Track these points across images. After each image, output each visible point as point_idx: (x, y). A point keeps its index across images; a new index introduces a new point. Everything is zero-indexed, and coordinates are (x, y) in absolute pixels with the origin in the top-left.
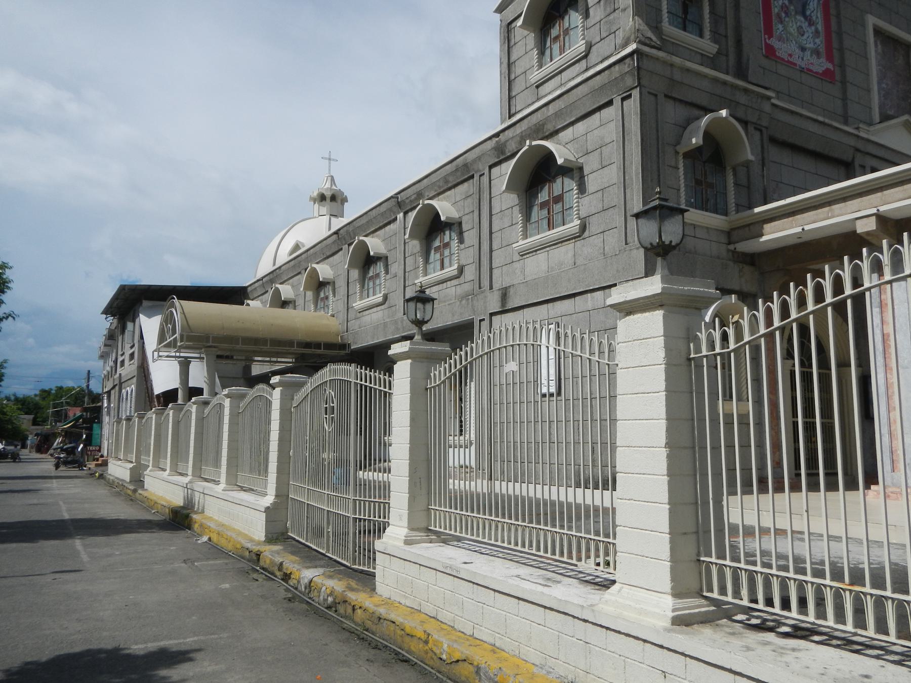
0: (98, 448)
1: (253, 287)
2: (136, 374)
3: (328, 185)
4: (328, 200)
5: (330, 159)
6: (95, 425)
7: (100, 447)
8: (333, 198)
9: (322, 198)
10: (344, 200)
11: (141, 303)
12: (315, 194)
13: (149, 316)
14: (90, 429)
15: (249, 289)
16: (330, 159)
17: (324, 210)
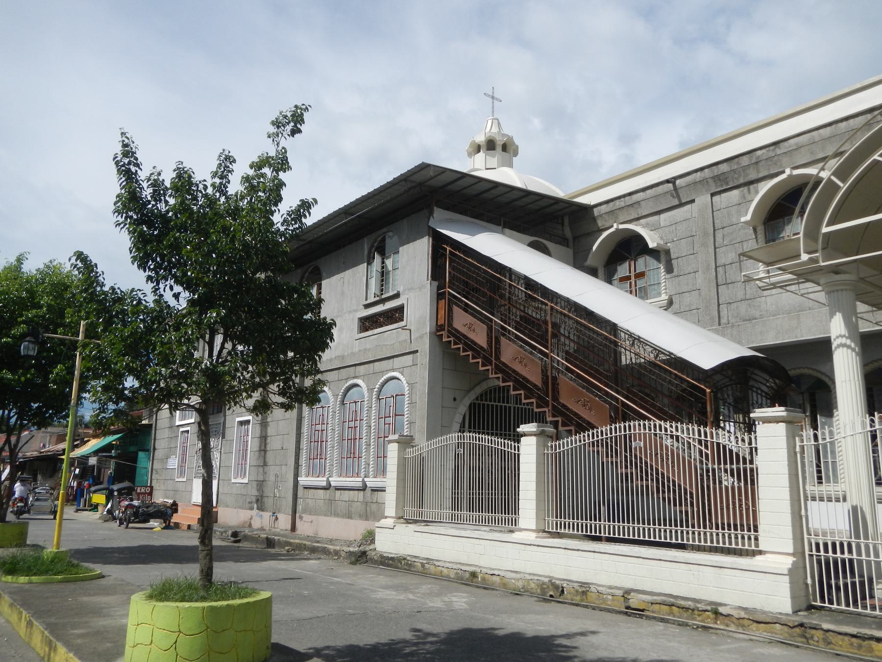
0: (148, 490)
1: (604, 208)
2: (424, 345)
3: (495, 130)
4: (499, 148)
5: (493, 97)
6: (141, 455)
7: (151, 487)
8: (505, 148)
9: (491, 145)
10: (516, 154)
11: (431, 213)
12: (481, 139)
13: (473, 235)
14: (135, 460)
15: (596, 211)
16: (493, 97)
17: (493, 161)
